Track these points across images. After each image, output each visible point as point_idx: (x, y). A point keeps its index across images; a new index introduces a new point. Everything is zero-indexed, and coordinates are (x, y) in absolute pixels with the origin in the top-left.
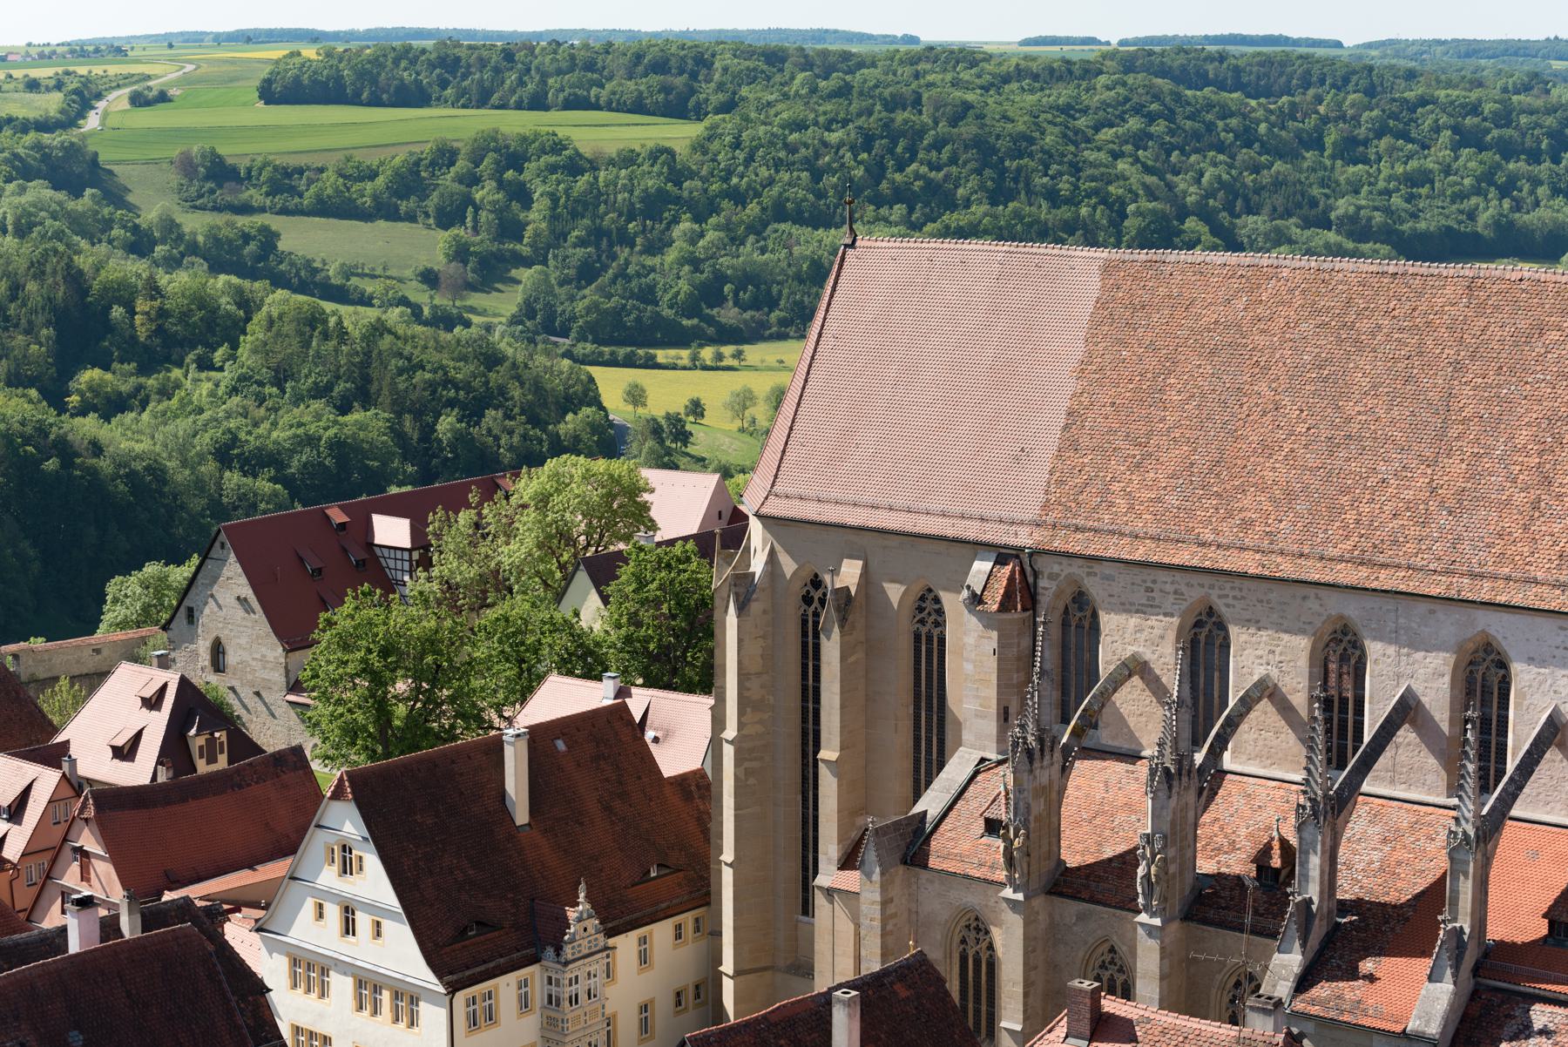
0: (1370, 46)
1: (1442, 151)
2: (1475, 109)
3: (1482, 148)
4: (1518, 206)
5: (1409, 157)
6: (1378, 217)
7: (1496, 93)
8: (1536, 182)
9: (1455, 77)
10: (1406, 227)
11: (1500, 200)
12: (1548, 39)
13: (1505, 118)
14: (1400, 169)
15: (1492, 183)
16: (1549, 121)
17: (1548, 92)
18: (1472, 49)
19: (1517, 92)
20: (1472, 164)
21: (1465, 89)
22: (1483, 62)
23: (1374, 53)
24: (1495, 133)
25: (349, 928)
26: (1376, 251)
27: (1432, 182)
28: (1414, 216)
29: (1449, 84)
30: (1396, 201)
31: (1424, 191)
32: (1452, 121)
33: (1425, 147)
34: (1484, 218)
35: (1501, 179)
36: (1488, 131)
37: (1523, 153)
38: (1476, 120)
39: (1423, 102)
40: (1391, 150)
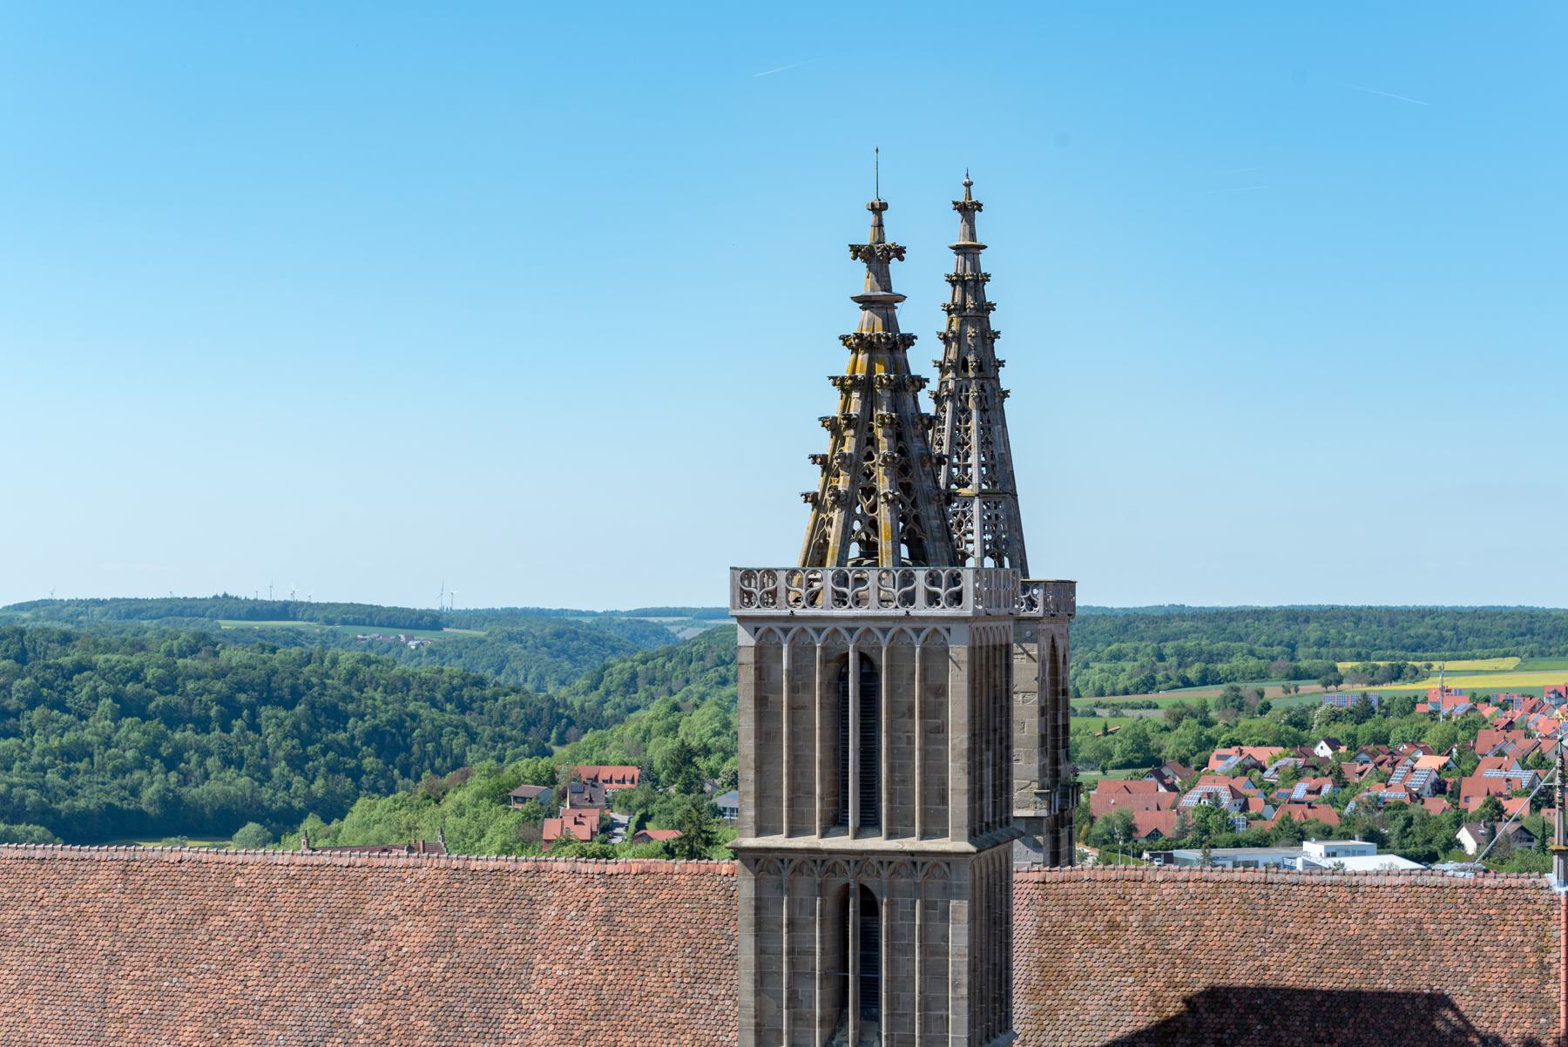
0: (21, 607)
1: (100, 721)
2: (136, 675)
3: (145, 717)
4: (184, 782)
5: (65, 729)
6: (33, 796)
7: (160, 658)
8: (205, 753)
9: (115, 640)
10: (61, 806)
11: (166, 773)
12: (216, 597)
13: (168, 684)
14: (55, 742)
15: (156, 755)
16: (218, 686)
17: (216, 654)
18: (133, 609)
19: (183, 655)
20: (135, 735)
21: (125, 653)
22: (145, 623)
23: (26, 615)
24: (160, 700)
26: (30, 833)
27: (91, 756)
28: (72, 793)
29: (109, 648)
30: (52, 777)
31: (82, 766)
32: (112, 689)
33: (82, 717)
34: (148, 793)
35: (165, 750)
36: (151, 698)
37: (191, 720)
38: (138, 687)
39: (80, 668)
40: (46, 721)
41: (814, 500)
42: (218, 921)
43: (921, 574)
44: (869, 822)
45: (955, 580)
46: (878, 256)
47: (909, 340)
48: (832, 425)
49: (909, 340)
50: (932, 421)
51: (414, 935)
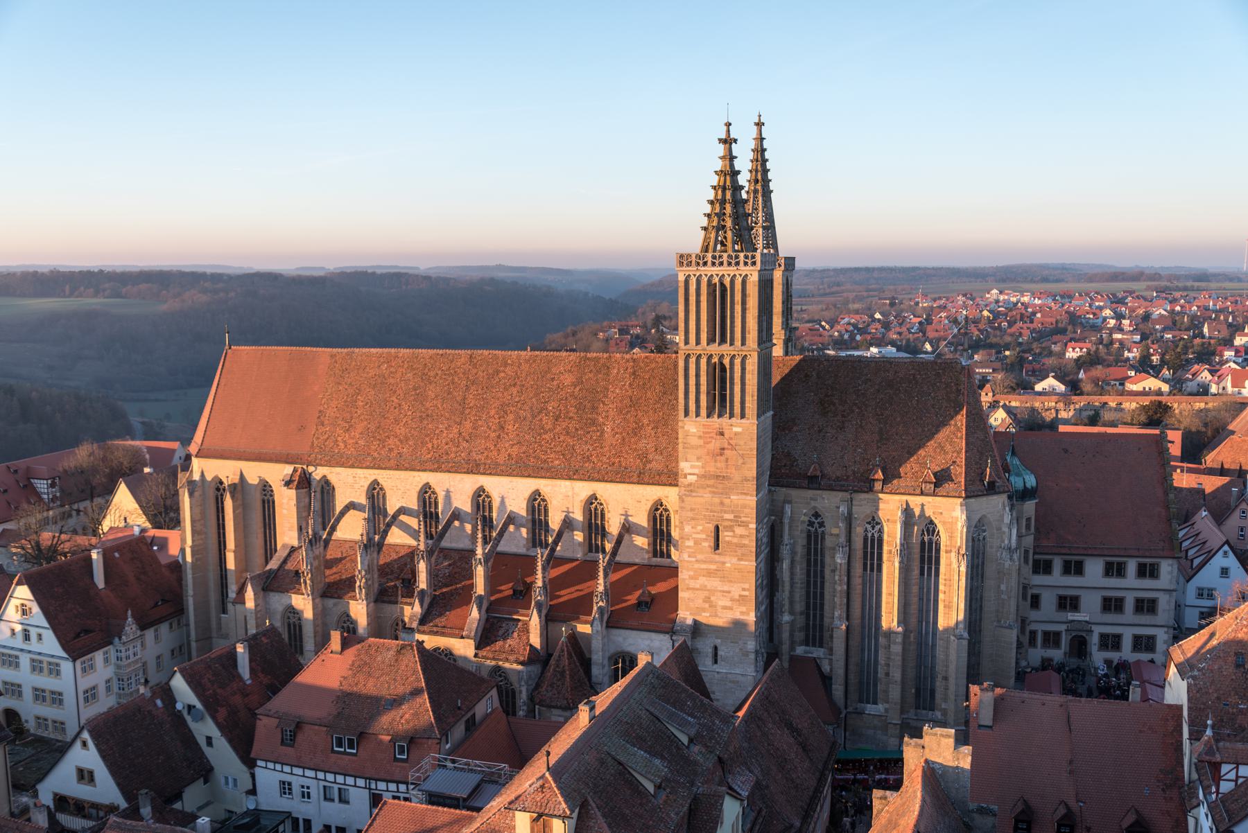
25: (27, 637)
41: (705, 229)
42: (502, 375)
43: (742, 255)
44: (723, 341)
45: (753, 257)
46: (728, 141)
47: (739, 172)
48: (711, 202)
49: (739, 172)
50: (746, 201)
51: (568, 379)
